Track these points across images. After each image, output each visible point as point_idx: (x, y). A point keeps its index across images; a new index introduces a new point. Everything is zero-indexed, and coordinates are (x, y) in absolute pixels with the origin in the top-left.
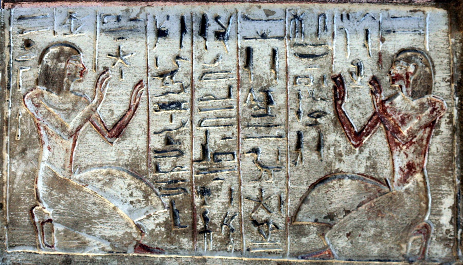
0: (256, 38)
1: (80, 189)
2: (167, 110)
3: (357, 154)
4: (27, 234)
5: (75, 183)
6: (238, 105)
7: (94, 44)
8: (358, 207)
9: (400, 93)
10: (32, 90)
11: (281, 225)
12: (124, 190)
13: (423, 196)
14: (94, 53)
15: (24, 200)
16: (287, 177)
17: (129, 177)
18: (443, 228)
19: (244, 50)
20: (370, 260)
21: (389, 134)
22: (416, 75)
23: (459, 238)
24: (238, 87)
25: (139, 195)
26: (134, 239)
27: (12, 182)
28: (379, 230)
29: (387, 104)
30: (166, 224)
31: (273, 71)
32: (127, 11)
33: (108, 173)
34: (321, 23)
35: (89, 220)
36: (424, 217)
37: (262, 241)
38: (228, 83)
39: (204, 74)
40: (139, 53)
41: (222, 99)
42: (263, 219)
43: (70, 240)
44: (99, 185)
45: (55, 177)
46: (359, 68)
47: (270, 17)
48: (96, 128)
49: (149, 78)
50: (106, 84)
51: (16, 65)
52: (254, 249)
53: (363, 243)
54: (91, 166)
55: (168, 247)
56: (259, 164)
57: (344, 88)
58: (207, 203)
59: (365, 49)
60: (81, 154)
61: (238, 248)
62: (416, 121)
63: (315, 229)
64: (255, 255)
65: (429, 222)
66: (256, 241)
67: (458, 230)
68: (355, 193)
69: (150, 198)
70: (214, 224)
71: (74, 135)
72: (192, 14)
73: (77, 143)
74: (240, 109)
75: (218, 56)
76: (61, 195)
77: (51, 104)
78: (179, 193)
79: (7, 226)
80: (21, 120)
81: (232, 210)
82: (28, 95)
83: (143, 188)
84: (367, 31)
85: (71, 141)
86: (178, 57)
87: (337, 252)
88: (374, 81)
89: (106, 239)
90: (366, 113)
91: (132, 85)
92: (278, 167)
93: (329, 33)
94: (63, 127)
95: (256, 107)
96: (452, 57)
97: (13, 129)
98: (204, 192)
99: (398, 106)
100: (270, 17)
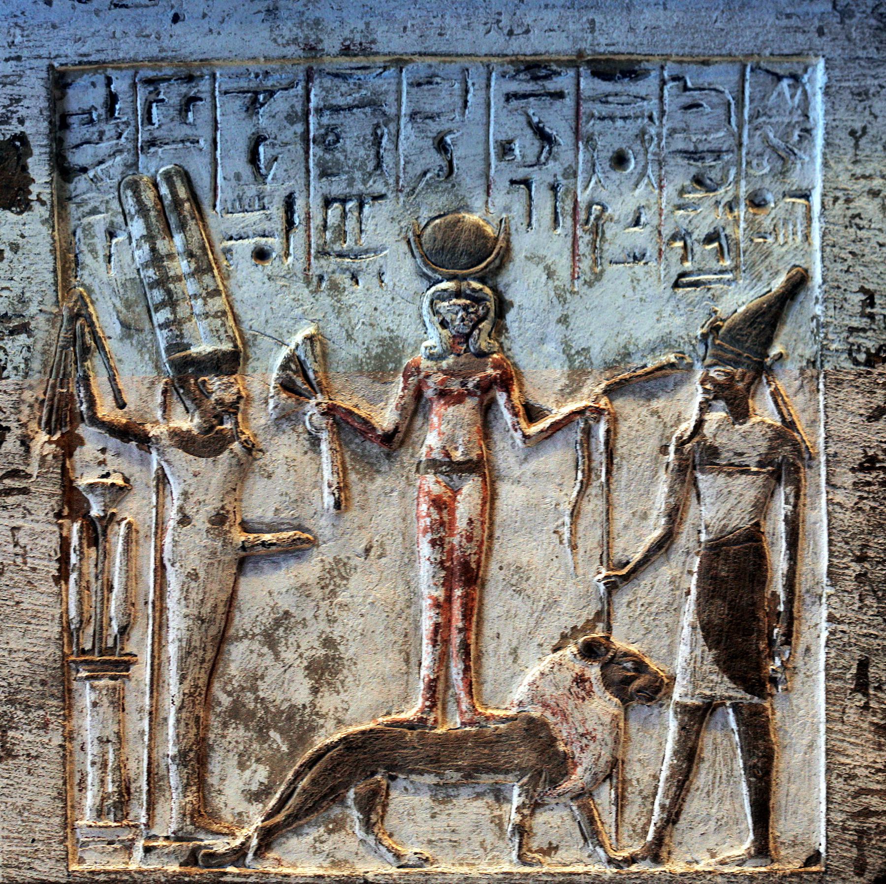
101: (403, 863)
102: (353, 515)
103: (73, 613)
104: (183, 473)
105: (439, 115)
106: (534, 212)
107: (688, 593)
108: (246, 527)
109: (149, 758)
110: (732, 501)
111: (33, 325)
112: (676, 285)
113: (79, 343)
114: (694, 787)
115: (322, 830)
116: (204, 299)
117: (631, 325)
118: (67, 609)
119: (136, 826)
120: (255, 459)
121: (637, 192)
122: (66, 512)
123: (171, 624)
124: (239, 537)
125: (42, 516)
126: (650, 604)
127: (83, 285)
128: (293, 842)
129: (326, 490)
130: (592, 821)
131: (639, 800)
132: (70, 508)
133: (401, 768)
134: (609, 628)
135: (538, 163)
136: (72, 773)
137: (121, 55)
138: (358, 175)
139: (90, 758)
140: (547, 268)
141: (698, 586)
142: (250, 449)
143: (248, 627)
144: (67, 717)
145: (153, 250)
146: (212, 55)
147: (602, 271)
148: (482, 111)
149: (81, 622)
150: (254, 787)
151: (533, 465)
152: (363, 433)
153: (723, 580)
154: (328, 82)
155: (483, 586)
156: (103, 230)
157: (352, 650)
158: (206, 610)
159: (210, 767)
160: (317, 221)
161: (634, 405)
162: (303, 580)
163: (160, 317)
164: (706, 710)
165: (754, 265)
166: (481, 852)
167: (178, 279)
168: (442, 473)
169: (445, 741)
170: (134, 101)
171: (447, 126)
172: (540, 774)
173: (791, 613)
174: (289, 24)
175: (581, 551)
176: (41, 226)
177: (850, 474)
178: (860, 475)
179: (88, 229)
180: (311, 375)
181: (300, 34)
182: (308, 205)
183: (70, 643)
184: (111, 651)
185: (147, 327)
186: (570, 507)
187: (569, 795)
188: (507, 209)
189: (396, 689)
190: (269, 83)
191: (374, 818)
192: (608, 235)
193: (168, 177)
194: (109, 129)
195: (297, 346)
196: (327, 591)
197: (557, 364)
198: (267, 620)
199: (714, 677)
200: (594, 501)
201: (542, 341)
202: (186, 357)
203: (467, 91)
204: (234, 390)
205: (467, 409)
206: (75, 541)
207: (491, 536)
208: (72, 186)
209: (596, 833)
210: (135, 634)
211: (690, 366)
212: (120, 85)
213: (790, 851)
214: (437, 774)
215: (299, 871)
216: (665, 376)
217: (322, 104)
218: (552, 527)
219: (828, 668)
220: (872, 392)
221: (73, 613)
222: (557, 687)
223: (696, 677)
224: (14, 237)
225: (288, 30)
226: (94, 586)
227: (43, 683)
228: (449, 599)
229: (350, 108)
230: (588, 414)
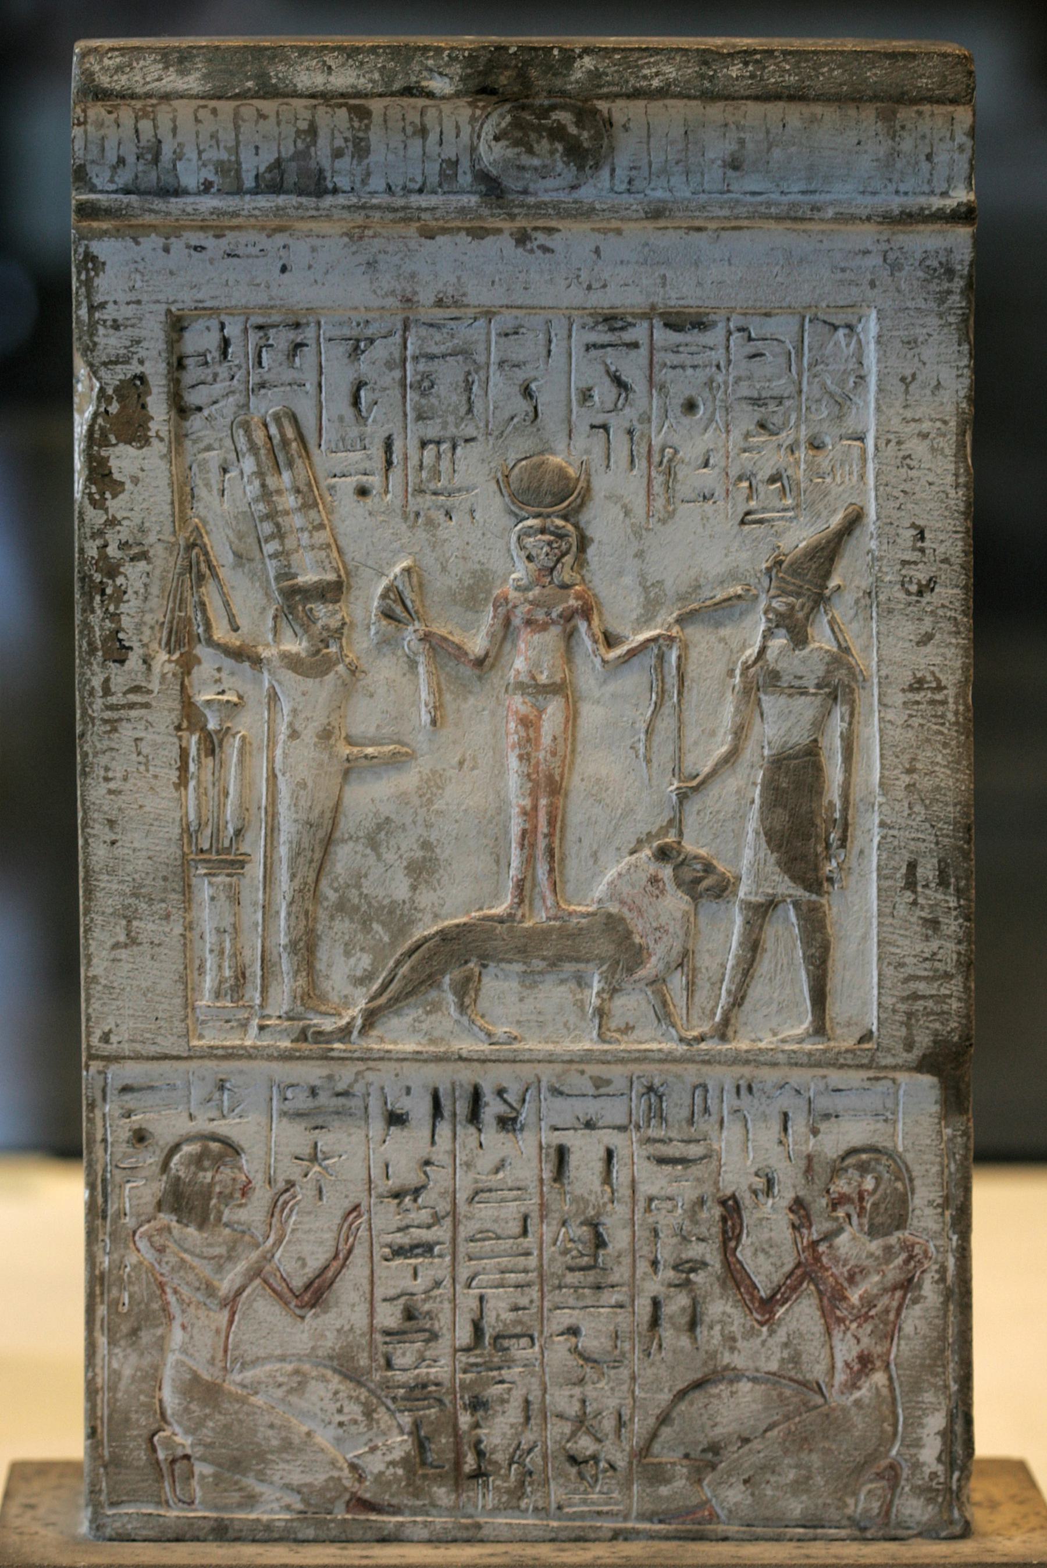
0: (575, 1129)
1: (243, 1401)
2: (406, 1258)
3: (763, 1337)
4: (143, 1481)
5: (233, 1388)
6: (541, 1249)
7: (269, 1138)
8: (766, 1431)
9: (848, 1228)
10: (149, 1221)
11: (621, 1463)
12: (326, 1401)
13: (887, 1413)
14: (268, 1153)
15: (138, 1420)
16: (633, 1378)
17: (336, 1379)
18: (925, 1468)
19: (552, 1151)
20: (787, 1526)
21: (825, 1301)
22: (877, 1196)
23: (954, 1487)
24: (542, 1218)
25: (354, 1410)
26: (346, 1489)
27: (113, 1388)
28: (803, 1472)
29: (822, 1248)
30: (405, 1462)
31: (607, 1188)
32: (330, 1077)
33: (297, 1372)
35: (261, 1456)
36: (889, 1450)
37: (585, 1492)
38: (523, 1209)
39: (476, 1193)
41: (510, 1238)
42: (588, 1453)
43: (226, 1491)
44: (280, 1393)
45: (196, 1378)
46: (770, 1183)
47: (602, 1091)
48: (274, 1290)
49: (373, 1200)
50: (291, 1211)
51: (119, 1176)
52: (570, 1506)
53: (773, 1496)
55: (410, 1503)
56: (581, 1355)
57: (740, 1217)
58: (481, 1423)
59: (781, 1148)
60: (244, 1338)
61: (540, 1505)
62: (876, 1278)
63: (685, 1470)
64: (573, 1517)
65: (899, 1458)
66: (575, 1492)
67: (952, 1473)
68: (760, 1407)
69: (375, 1416)
70: (496, 1462)
71: (231, 1303)
72: (453, 1084)
73: (237, 1317)
74: (545, 1256)
75: (503, 1160)
76: (207, 1411)
77: (186, 1246)
78: (429, 1407)
79: (105, 1467)
80: (129, 1276)
81: (529, 1437)
82: (142, 1229)
83: (362, 1398)
84: (786, 1115)
85: (226, 1314)
86: (427, 1163)
87: (726, 1512)
88: (798, 1205)
89: (292, 1489)
90: (783, 1265)
91: (339, 1213)
93: (714, 1118)
94: (210, 1290)
95: (574, 1253)
96: (946, 1162)
97: (115, 1292)
98: (477, 1405)
99: (843, 1251)
100: (602, 1091)
101: (494, 1040)
103: (192, 816)
106: (612, 455)
107: (753, 802)
108: (350, 741)
110: (793, 719)
111: (151, 554)
112: (743, 522)
113: (194, 570)
114: (757, 974)
115: (420, 1011)
116: (310, 532)
120: (358, 680)
122: (185, 725)
123: (282, 828)
124: (345, 750)
125: (162, 728)
126: (718, 812)
127: (198, 517)
130: (665, 1004)
131: (708, 985)
132: (189, 721)
134: (681, 834)
135: (615, 409)
136: (192, 960)
137: (233, 303)
138: (451, 419)
139: (208, 946)
140: (624, 506)
141: (761, 796)
142: (353, 671)
143: (352, 831)
144: (186, 910)
145: (263, 485)
147: (674, 510)
148: (563, 359)
150: (359, 973)
151: (611, 687)
152: (457, 658)
154: (423, 331)
155: (566, 795)
156: (217, 465)
158: (314, 816)
159: (319, 955)
160: (413, 462)
163: (270, 548)
166: (564, 1031)
167: (287, 513)
168: (529, 694)
170: (246, 346)
171: (533, 374)
172: (618, 963)
173: (846, 819)
174: (388, 276)
175: (655, 765)
176: (159, 461)
177: (901, 694)
178: (910, 695)
179: (203, 465)
181: (398, 286)
182: (405, 446)
183: (190, 843)
184: (228, 850)
185: (258, 556)
186: (644, 726)
187: (643, 983)
188: (588, 452)
190: (369, 332)
192: (680, 476)
193: (277, 418)
194: (223, 371)
196: (424, 799)
198: (369, 824)
199: (776, 877)
201: (620, 573)
202: (293, 586)
203: (550, 341)
204: (339, 617)
206: (193, 752)
207: (573, 751)
208: (188, 424)
209: (668, 1015)
210: (249, 836)
211: (756, 597)
212: (233, 331)
213: (845, 1030)
214: (525, 963)
215: (400, 1047)
216: (732, 606)
217: (417, 352)
218: (629, 743)
221: (192, 816)
222: (633, 886)
223: (759, 878)
224: (134, 470)
225: (387, 282)
226: (211, 792)
227: (165, 879)
228: (535, 808)
229: (444, 356)
230: (661, 641)
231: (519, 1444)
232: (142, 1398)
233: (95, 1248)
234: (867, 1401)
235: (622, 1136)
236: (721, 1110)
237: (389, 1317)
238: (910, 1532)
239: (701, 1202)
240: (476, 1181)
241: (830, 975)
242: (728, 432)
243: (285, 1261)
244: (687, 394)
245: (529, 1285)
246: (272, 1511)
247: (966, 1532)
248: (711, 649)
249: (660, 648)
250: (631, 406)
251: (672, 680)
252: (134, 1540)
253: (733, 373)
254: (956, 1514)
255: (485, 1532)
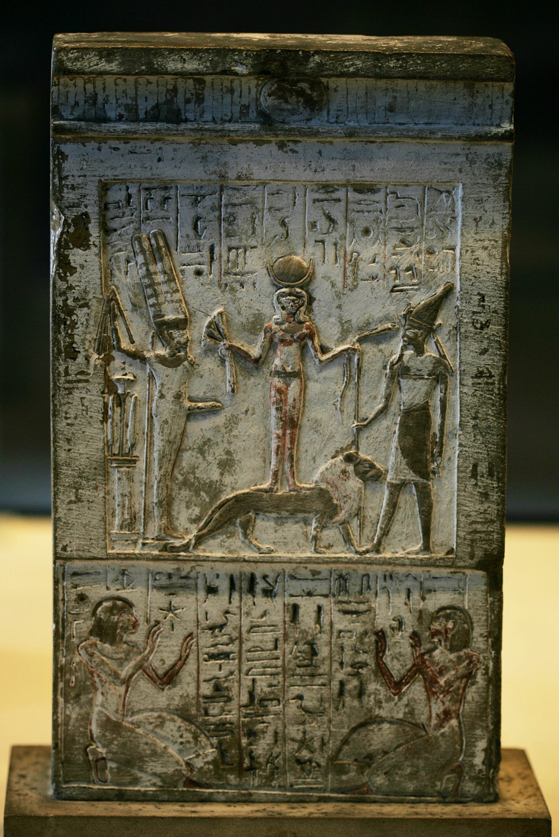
0: (302, 596)
2: (216, 660)
5: (127, 725)
6: (284, 656)
7: (146, 599)
8: (396, 748)
9: (440, 647)
10: (85, 640)
12: (174, 731)
14: (146, 607)
15: (79, 740)
16: (330, 721)
19: (290, 607)
20: (406, 796)
23: (491, 776)
24: (285, 640)
25: (188, 736)
26: (184, 775)
27: (66, 724)
29: (426, 657)
31: (318, 626)
32: (178, 569)
33: (159, 717)
34: (365, 582)
35: (141, 758)
36: (459, 758)
37: (305, 778)
38: (275, 636)
40: (190, 608)
41: (268, 650)
42: (306, 758)
43: (123, 776)
44: (151, 727)
45: (108, 719)
46: (401, 623)
47: (316, 577)
50: (158, 635)
52: (297, 785)
54: (143, 710)
55: (216, 783)
61: (282, 784)
62: (453, 672)
63: (355, 767)
66: (300, 778)
67: (490, 770)
69: (199, 739)
72: (240, 573)
73: (130, 689)
74: (286, 660)
76: (114, 736)
78: (226, 735)
79: (62, 763)
81: (277, 750)
82: (82, 645)
83: (193, 730)
86: (227, 612)
88: (415, 636)
90: (406, 665)
91: (182, 637)
92: (321, 713)
93: (373, 591)
94: (116, 675)
95: (301, 658)
96: (489, 614)
97: (68, 676)
99: (436, 658)
101: (262, 551)
102: (240, 396)
104: (161, 375)
105: (282, 209)
107: (395, 433)
108: (191, 399)
109: (145, 503)
111: (90, 303)
112: (392, 291)
114: (396, 519)
116: (171, 294)
117: (370, 310)
118: (107, 436)
119: (138, 534)
121: (374, 247)
122: (106, 391)
123: (155, 443)
125: (95, 393)
126: (377, 438)
127: (114, 285)
128: (211, 542)
129: (228, 384)
130: (348, 534)
131: (370, 525)
133: (261, 510)
134: (358, 448)
135: (328, 233)
136: (109, 510)
137: (133, 176)
139: (117, 503)
140: (332, 282)
141: (399, 430)
142: (192, 364)
143: (191, 445)
145: (148, 270)
146: (177, 178)
147: (357, 284)
149: (113, 441)
153: (411, 428)
154: (230, 192)
155: (300, 428)
156: (124, 259)
157: (239, 456)
159: (173, 507)
160: (225, 258)
161: (371, 347)
162: (216, 424)
163: (151, 301)
164: (402, 486)
165: (428, 281)
167: (159, 284)
168: (282, 377)
169: (281, 498)
171: (286, 214)
172: (325, 513)
173: (442, 442)
175: (345, 413)
176: (94, 257)
178: (476, 380)
179: (117, 259)
180: (221, 330)
182: (220, 250)
184: (127, 455)
185: (144, 306)
186: (340, 393)
189: (259, 474)
190: (202, 192)
191: (248, 532)
192: (360, 267)
193: (155, 235)
194: (127, 211)
195: (215, 317)
197: (336, 327)
198: (199, 442)
199: (405, 471)
200: (352, 391)
201: (329, 316)
202: (162, 321)
203: (295, 198)
204: (185, 337)
205: (294, 348)
206: (110, 405)
207: (304, 406)
208: (109, 238)
210: (139, 447)
211: (398, 329)
212: (133, 190)
213: (440, 548)
214: (278, 513)
215: (214, 555)
218: (333, 402)
219: (459, 467)
220: (482, 342)
221: (109, 437)
222: (333, 475)
223: (397, 471)
224: (82, 261)
225: (212, 167)
226: (119, 425)
227: (95, 469)
228: (284, 434)
229: (241, 205)
231: (272, 753)
232: (81, 729)
233: (58, 654)
234: (447, 734)
235: (326, 600)
236: (376, 587)
237: (207, 689)
238: (468, 799)
239: (366, 633)
240: (252, 622)
241: (433, 520)
242: (385, 245)
243: (154, 661)
244: (364, 225)
245: (278, 674)
246: (146, 786)
247: (496, 799)
248: (375, 355)
249: (349, 354)
250: (336, 231)
251: (354, 371)
252: (77, 800)
253: (389, 215)
254: (491, 790)
255: (254, 797)
